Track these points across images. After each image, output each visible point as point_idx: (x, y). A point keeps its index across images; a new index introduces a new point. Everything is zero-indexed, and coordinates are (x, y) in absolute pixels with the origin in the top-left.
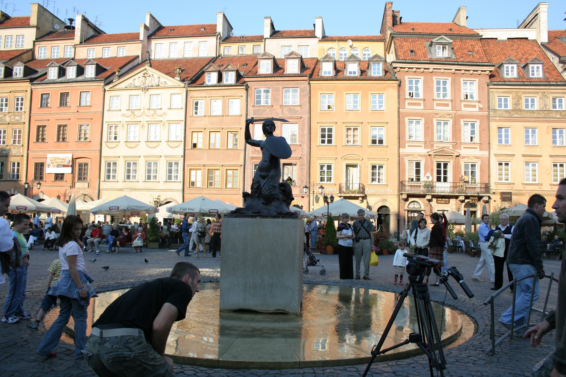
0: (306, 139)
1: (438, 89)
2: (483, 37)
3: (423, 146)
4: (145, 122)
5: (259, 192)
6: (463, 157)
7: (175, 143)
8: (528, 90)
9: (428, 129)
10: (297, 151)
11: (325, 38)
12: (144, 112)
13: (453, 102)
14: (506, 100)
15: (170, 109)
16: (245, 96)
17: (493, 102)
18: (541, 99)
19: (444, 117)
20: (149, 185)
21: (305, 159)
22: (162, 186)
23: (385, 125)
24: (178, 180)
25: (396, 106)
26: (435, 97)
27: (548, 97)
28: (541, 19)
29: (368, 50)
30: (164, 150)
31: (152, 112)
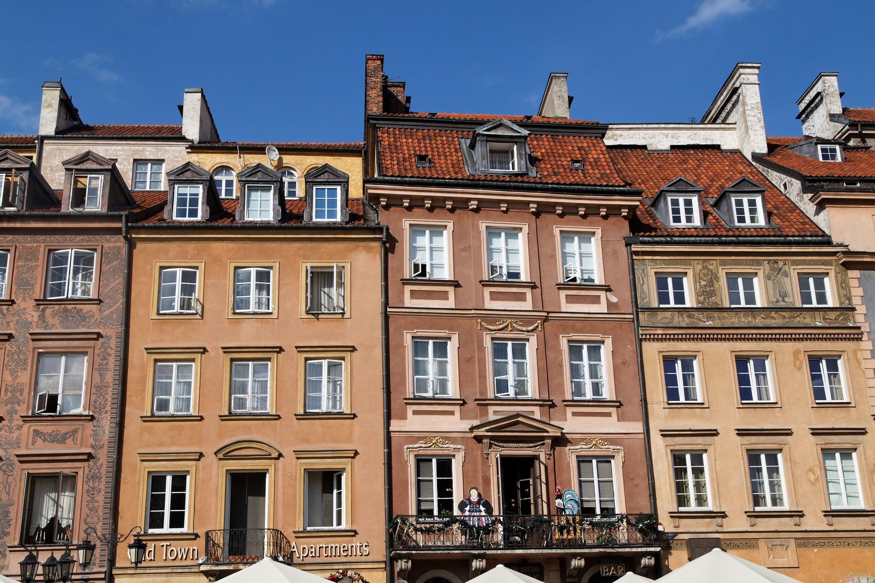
10: (79, 435)
13: (538, 291)
14: (678, 285)
17: (645, 287)
18: (768, 277)
23: (347, 355)
25: (379, 298)
27: (786, 275)
28: (748, 102)
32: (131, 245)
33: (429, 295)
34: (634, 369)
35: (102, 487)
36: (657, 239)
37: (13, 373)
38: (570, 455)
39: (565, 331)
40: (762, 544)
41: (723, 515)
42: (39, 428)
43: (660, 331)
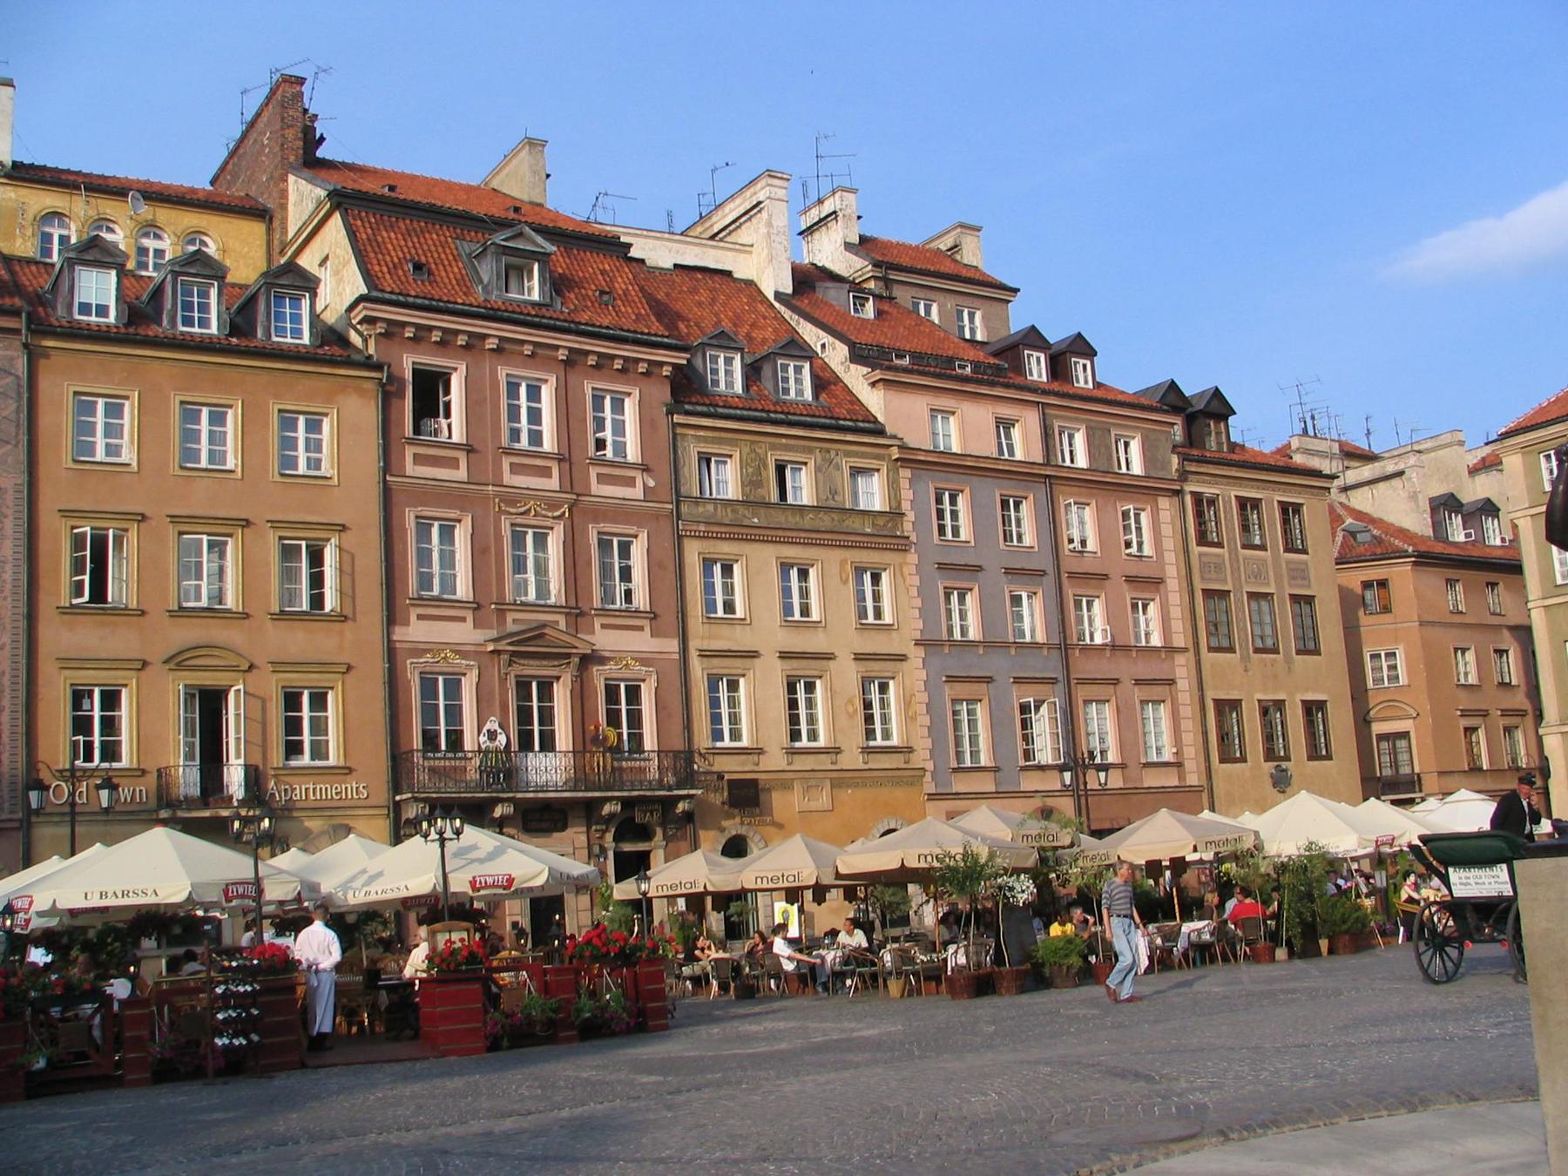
2: (634, 253)
6: (603, 660)
17: (686, 470)
18: (818, 469)
27: (838, 467)
32: (34, 356)
34: (671, 576)
36: (699, 408)
38: (598, 677)
41: (760, 751)
43: (702, 528)
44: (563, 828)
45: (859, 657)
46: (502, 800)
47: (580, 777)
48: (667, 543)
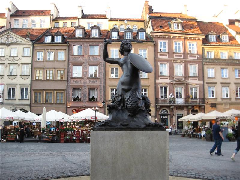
0: (103, 74)
1: (176, 47)
2: (198, 21)
3: (168, 79)
4: (8, 64)
5: (122, 104)
6: (190, 84)
7: (26, 77)
8: (222, 49)
9: (171, 69)
10: (98, 81)
11: (112, 20)
12: (7, 58)
13: (184, 55)
15: (22, 56)
16: (67, 49)
19: (179, 62)
20: (10, 102)
21: (102, 85)
22: (17, 102)
24: (28, 98)
26: (175, 52)
27: (232, 52)
29: (136, 26)
30: (19, 81)
31: (12, 58)
33: (163, 55)
35: (102, 91)
37: (85, 69)
39: (189, 63)
40: (224, 105)
41: (217, 99)
42: (91, 80)
44: (183, 110)
45: (235, 84)
46: (172, 105)
47: (186, 101)
48: (201, 66)
